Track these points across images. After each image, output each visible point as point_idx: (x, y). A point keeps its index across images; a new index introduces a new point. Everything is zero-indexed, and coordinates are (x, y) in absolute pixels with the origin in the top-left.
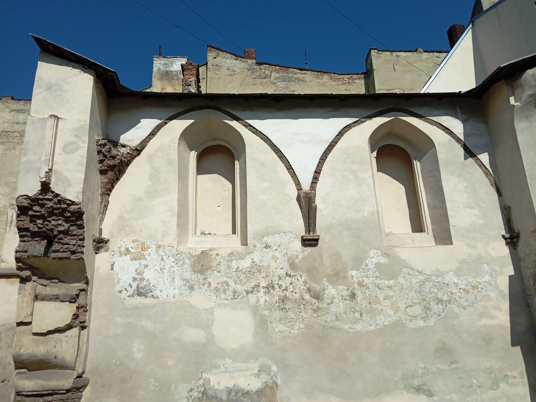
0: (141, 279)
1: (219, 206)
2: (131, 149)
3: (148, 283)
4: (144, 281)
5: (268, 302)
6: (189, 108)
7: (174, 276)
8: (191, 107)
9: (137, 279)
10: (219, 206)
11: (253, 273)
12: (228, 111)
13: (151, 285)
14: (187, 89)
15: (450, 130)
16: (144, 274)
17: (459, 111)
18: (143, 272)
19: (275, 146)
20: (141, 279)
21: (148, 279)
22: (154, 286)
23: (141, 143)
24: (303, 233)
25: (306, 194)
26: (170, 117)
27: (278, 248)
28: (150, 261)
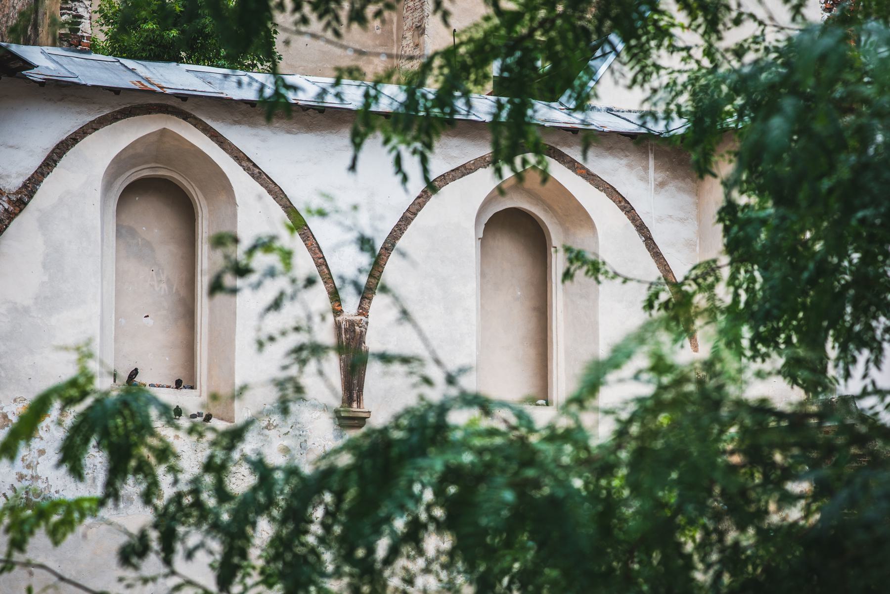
0: (32, 477)
1: (147, 316)
2: (10, 201)
3: (46, 485)
4: (39, 481)
5: (267, 533)
6: (123, 107)
7: (95, 474)
8: (128, 106)
9: (26, 476)
10: (147, 316)
11: (242, 477)
12: (200, 117)
13: (53, 490)
14: (70, 9)
15: (629, 203)
16: (39, 468)
17: (651, 163)
18: (36, 463)
19: (294, 212)
20: (32, 477)
21: (47, 478)
22: (57, 492)
23: (25, 186)
24: (336, 404)
25: (352, 324)
26: (83, 127)
27: (289, 429)
28: (50, 443)
